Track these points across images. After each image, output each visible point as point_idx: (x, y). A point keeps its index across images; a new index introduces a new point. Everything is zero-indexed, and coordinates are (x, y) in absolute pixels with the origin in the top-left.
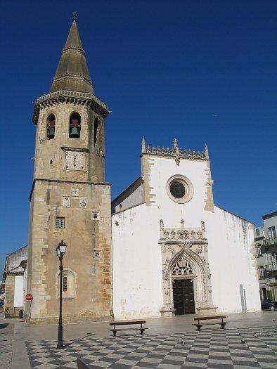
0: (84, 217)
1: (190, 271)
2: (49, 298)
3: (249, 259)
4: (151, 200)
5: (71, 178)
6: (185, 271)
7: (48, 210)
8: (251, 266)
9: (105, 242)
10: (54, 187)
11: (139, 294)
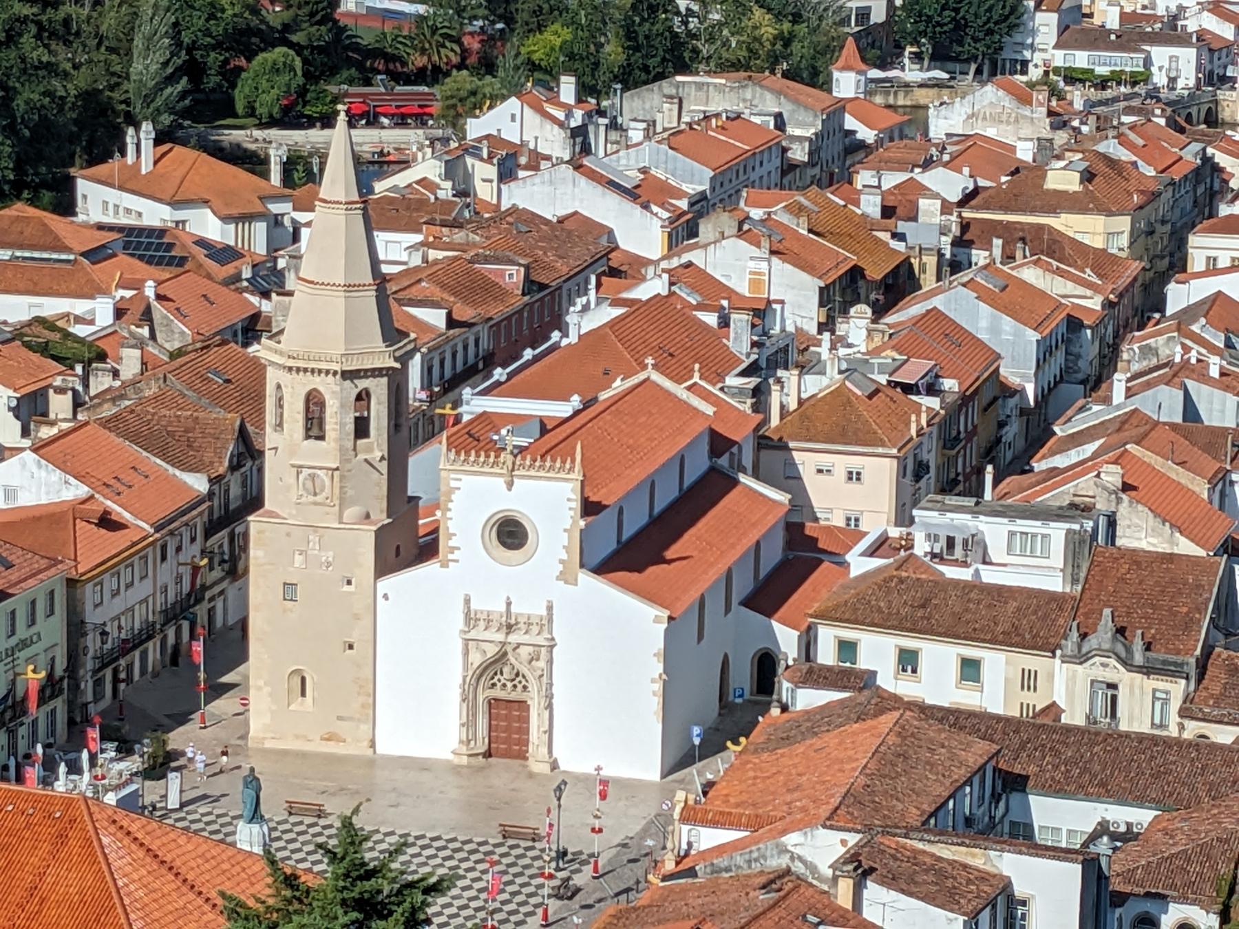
4: (450, 557)
6: (515, 686)
11: (419, 719)
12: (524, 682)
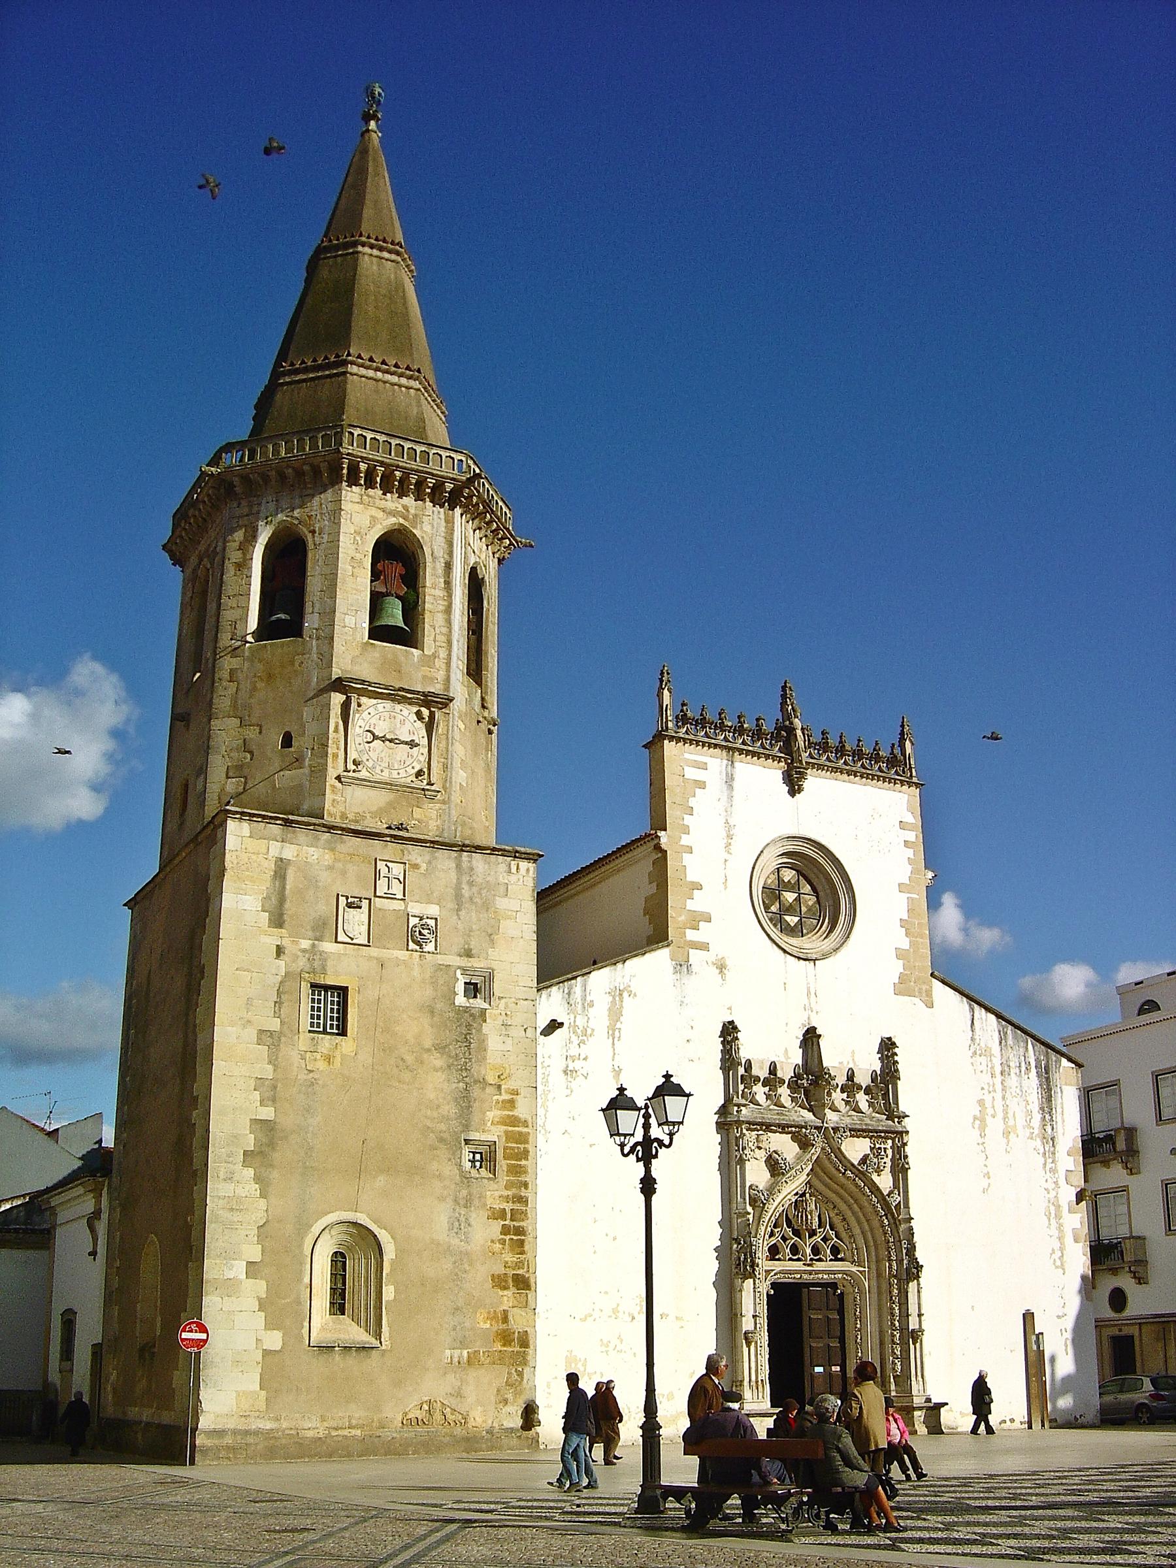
0: (429, 992)
2: (274, 1340)
3: (1058, 1208)
4: (691, 935)
5: (378, 814)
7: (280, 951)
8: (1069, 1239)
9: (511, 1104)
10: (307, 852)
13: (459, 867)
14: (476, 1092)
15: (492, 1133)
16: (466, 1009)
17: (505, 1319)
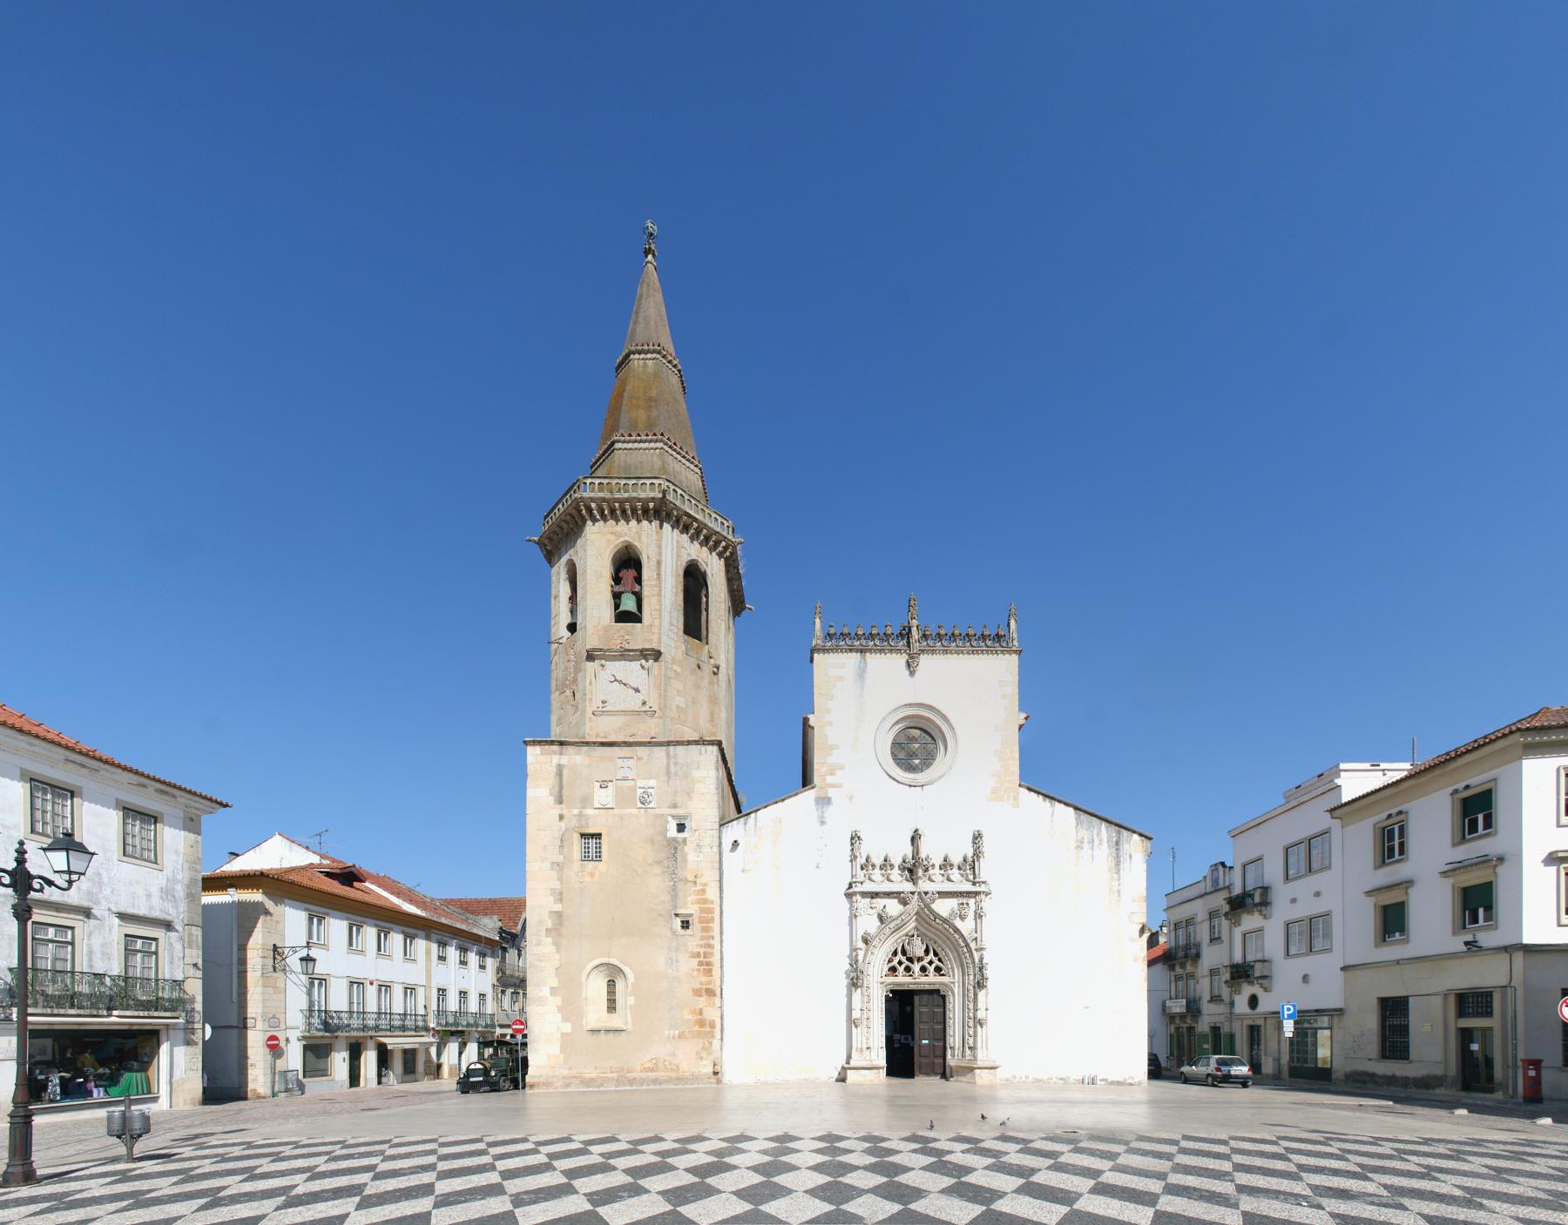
1: (938, 969)
2: (567, 1028)
4: (829, 779)
7: (561, 817)
9: (703, 891)
12: (937, 963)
13: (668, 754)
14: (680, 886)
15: (690, 909)
16: (674, 839)
17: (701, 1013)
